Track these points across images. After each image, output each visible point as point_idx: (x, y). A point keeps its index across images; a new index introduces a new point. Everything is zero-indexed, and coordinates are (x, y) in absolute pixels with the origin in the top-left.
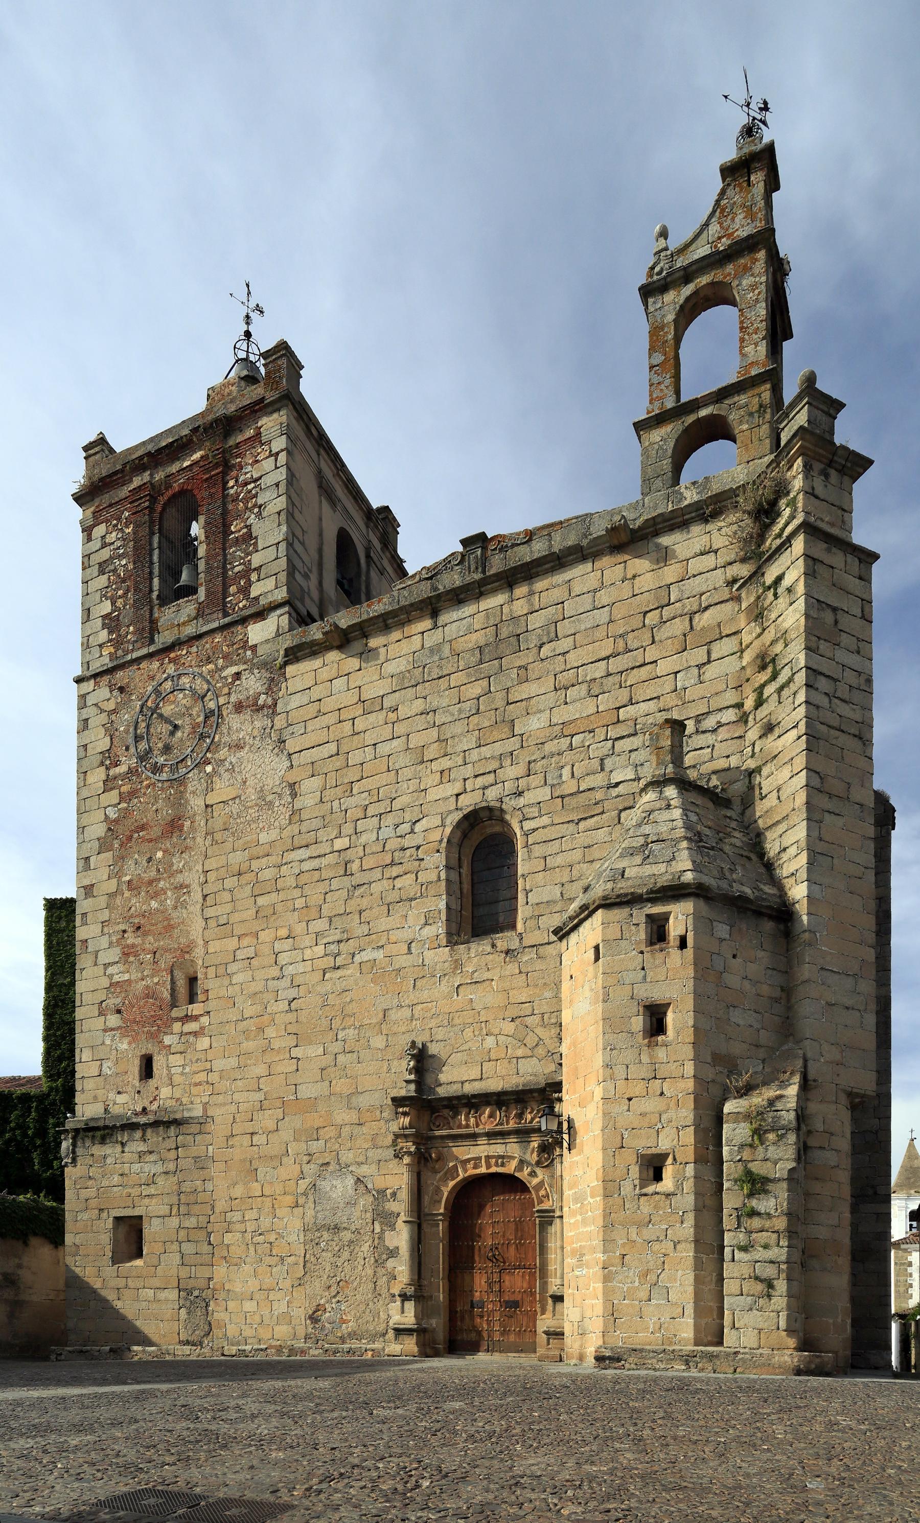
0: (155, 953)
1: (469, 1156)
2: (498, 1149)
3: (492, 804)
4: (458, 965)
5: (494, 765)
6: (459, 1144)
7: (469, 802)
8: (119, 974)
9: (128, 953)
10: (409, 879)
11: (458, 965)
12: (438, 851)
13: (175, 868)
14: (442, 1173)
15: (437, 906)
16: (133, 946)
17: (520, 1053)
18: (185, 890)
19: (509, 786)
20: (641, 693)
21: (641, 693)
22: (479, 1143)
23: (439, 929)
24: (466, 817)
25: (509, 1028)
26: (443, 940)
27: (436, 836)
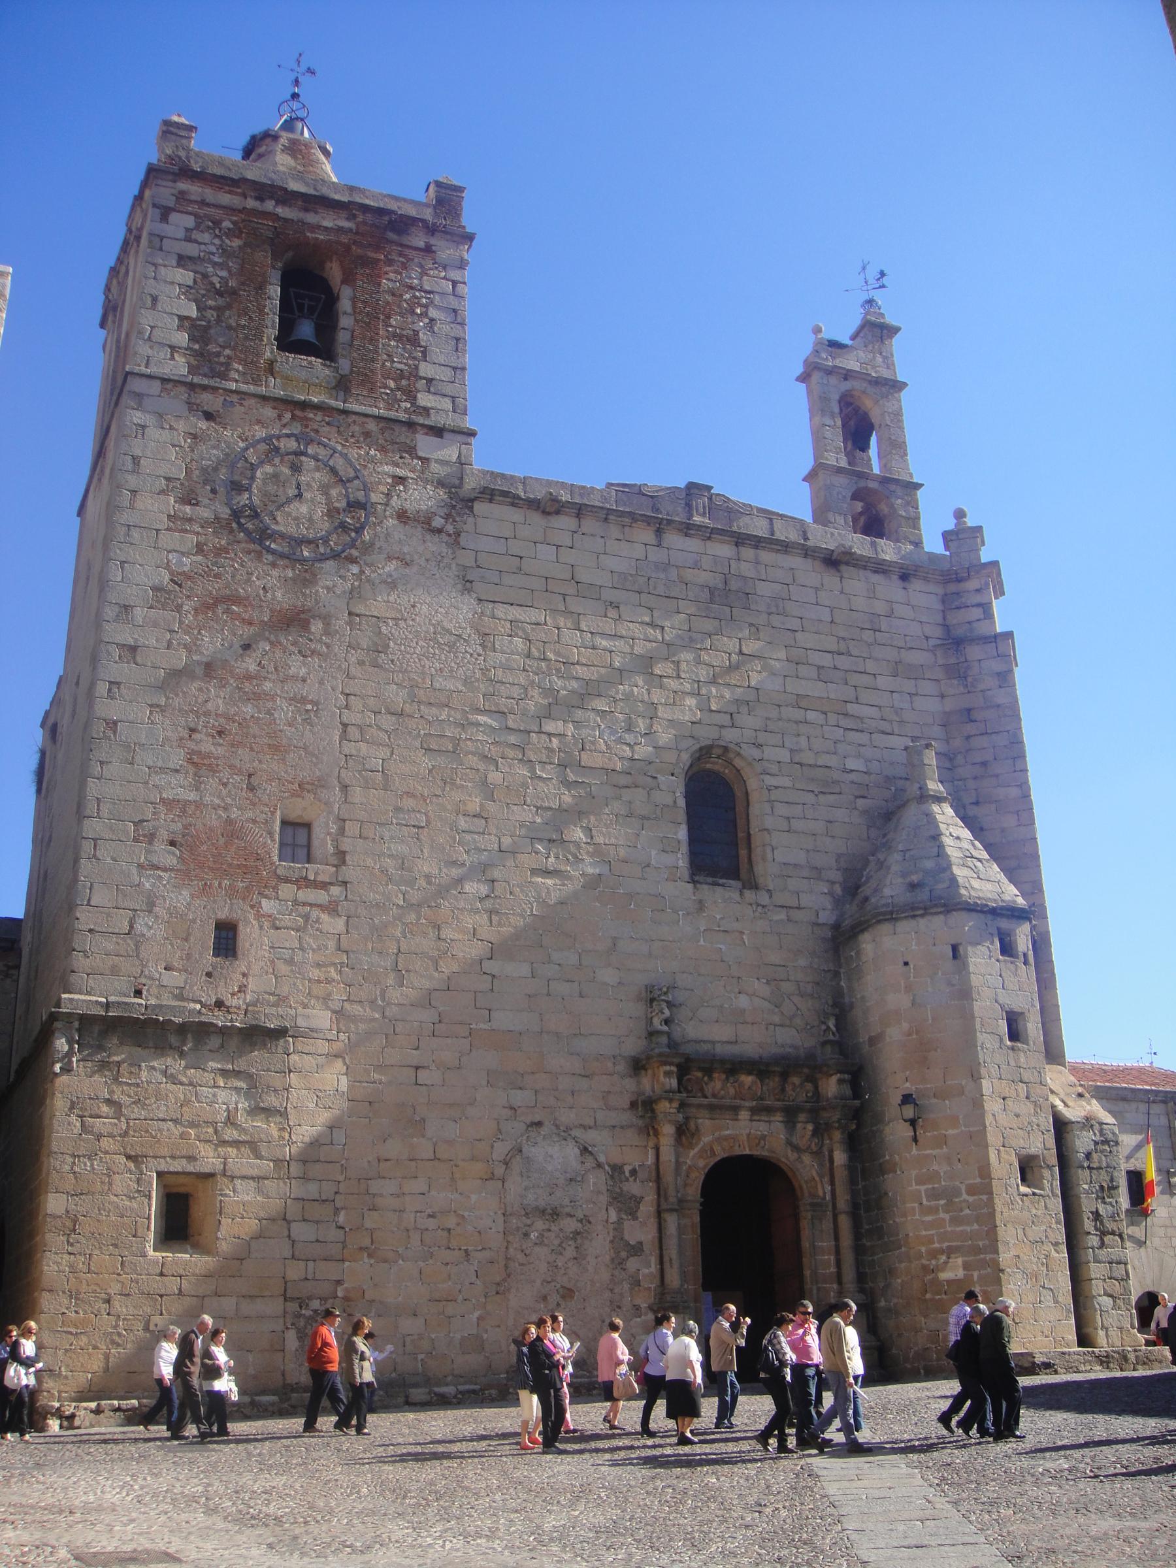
0: (250, 776)
1: (727, 1132)
2: (761, 1128)
3: (731, 746)
4: (701, 906)
5: (733, 709)
6: (717, 1116)
7: (707, 735)
8: (178, 788)
9: (199, 764)
10: (640, 794)
11: (701, 906)
12: (672, 775)
13: (291, 672)
14: (696, 1150)
15: (675, 834)
16: (209, 755)
17: (776, 1019)
18: (309, 707)
19: (748, 734)
20: (865, 696)
21: (865, 696)
22: (740, 1117)
23: (682, 860)
24: (701, 749)
25: (765, 990)
26: (686, 874)
27: (671, 757)
